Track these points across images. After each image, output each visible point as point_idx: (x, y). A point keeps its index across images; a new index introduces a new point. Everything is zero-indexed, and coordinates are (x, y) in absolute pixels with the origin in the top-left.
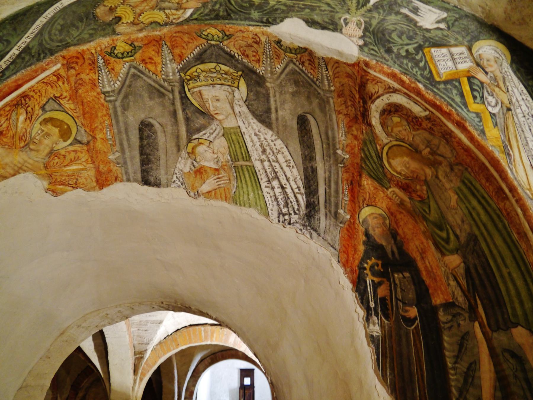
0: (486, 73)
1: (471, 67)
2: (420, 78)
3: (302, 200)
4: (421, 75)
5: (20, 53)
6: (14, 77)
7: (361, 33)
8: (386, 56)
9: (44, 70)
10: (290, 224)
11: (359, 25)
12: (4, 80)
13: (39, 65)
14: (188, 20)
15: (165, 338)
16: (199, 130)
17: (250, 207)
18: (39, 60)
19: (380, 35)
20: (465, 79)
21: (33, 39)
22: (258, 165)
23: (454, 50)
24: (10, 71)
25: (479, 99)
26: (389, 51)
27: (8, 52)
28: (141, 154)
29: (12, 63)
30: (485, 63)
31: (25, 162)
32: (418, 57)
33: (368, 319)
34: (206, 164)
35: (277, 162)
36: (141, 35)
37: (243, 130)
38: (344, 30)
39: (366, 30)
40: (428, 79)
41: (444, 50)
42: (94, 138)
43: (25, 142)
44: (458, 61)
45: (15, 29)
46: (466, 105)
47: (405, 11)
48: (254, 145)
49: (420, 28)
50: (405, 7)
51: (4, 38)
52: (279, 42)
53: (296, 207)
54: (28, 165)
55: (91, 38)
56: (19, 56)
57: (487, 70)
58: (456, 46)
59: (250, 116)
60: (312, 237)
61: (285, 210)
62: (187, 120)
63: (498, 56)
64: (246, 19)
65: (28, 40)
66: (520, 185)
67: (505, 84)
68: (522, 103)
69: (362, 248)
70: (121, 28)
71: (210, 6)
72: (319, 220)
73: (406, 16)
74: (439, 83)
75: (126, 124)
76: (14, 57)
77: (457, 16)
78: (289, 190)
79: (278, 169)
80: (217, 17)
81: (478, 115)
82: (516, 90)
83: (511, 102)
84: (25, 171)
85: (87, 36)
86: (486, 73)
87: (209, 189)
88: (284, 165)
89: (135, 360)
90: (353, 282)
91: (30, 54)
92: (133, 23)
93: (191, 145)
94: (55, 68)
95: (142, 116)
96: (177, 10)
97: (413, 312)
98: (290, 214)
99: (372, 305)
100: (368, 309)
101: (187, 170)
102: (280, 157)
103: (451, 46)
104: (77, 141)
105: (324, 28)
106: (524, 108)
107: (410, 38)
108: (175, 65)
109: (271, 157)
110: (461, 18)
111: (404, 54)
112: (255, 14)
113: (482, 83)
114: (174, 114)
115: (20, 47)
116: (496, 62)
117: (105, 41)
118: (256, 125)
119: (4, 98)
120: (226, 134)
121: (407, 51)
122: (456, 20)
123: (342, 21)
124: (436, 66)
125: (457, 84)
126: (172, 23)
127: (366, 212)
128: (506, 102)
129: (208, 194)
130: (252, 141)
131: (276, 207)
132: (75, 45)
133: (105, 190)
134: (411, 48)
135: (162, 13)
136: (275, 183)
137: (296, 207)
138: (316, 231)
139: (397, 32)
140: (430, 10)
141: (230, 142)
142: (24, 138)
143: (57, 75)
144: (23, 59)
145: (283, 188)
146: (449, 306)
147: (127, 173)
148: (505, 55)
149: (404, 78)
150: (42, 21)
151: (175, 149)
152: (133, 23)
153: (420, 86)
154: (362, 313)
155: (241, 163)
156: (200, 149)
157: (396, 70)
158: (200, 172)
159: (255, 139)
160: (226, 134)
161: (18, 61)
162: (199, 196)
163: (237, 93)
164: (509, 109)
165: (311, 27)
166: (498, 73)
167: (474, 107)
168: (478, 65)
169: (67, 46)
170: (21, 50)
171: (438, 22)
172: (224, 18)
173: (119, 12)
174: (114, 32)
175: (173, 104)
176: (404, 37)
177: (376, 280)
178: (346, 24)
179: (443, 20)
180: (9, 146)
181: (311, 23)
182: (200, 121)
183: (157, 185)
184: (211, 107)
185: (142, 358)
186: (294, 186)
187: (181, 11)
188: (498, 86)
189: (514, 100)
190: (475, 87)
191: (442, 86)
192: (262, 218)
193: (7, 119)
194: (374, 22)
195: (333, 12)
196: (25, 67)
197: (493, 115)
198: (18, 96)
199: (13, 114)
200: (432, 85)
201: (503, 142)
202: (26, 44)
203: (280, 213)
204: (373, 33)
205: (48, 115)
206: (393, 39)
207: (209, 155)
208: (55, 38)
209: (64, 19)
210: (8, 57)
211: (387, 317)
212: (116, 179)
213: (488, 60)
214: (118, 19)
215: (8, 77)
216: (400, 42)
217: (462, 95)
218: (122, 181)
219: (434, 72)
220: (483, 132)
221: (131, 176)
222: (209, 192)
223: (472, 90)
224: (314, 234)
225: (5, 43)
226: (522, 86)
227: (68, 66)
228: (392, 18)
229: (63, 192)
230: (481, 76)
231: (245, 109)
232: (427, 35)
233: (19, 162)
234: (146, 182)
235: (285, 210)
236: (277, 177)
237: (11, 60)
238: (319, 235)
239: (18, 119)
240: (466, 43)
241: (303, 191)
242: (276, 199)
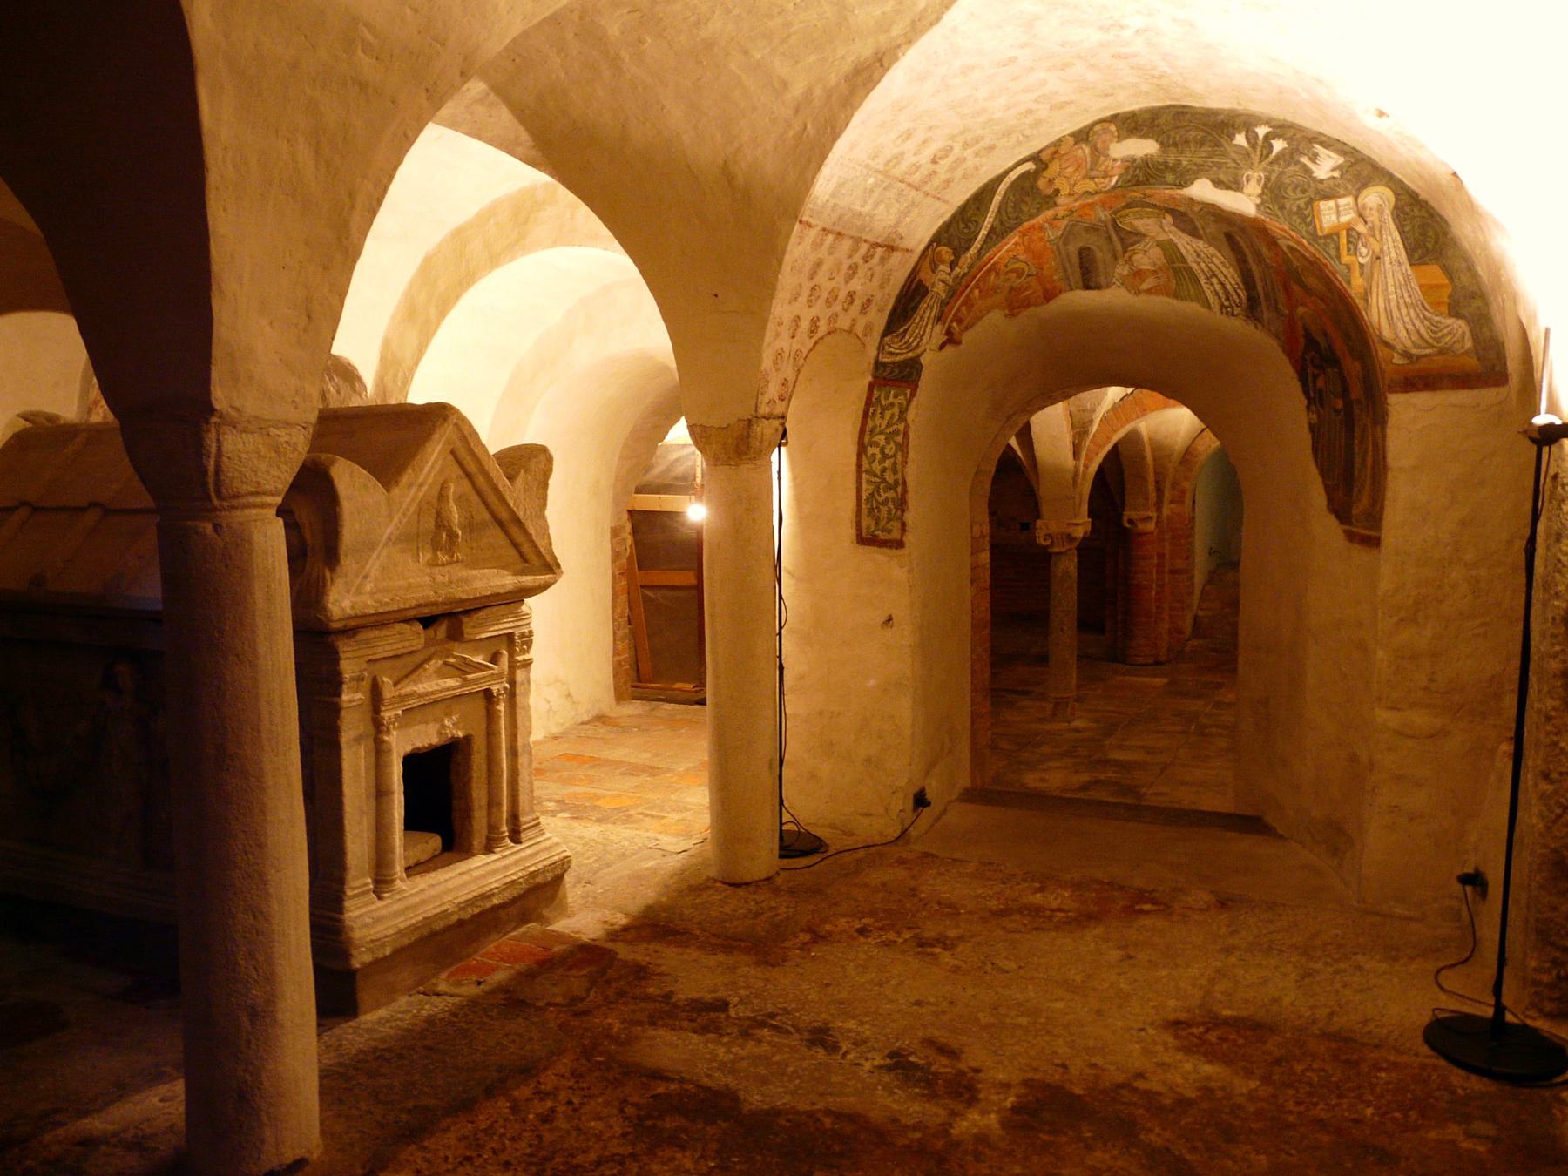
0: (1366, 222)
1: (1352, 219)
2: (1304, 234)
3: (1243, 294)
4: (1307, 232)
5: (989, 233)
6: (988, 255)
7: (1259, 190)
8: (1279, 213)
9: (1006, 244)
10: (1233, 315)
11: (1259, 181)
13: (1005, 240)
14: (1114, 188)
15: (1122, 399)
16: (1133, 245)
17: (1192, 301)
18: (1003, 238)
19: (1276, 191)
20: (1344, 232)
21: (994, 220)
22: (1194, 266)
23: (1342, 201)
25: (1352, 252)
26: (1282, 208)
27: (978, 233)
28: (1081, 268)
29: (985, 242)
30: (1367, 212)
32: (1306, 212)
33: (1308, 408)
34: (1143, 267)
35: (1213, 262)
36: (1077, 204)
37: (1176, 241)
38: (1245, 190)
39: (1265, 187)
40: (1311, 235)
41: (1331, 203)
42: (1042, 269)
44: (1342, 213)
45: (978, 209)
46: (1339, 257)
47: (1304, 160)
48: (1188, 251)
49: (1314, 179)
50: (1305, 154)
52: (1191, 199)
53: (1238, 301)
55: (1039, 211)
56: (988, 236)
57: (1368, 220)
58: (1344, 196)
59: (1181, 233)
60: (1256, 328)
61: (1226, 303)
62: (1121, 240)
63: (1381, 202)
64: (1161, 184)
65: (991, 220)
66: (1372, 325)
67: (1381, 231)
68: (1392, 250)
69: (1302, 340)
70: (1061, 200)
71: (1131, 173)
72: (1262, 311)
73: (1305, 165)
74: (1321, 237)
75: (1068, 255)
77: (1353, 160)
78: (1228, 287)
79: (1214, 268)
80: (1138, 183)
81: (1348, 267)
82: (1390, 238)
83: (1382, 250)
85: (1035, 211)
86: (1366, 222)
87: (1149, 286)
88: (1220, 266)
89: (1074, 436)
90: (1297, 371)
91: (995, 233)
92: (1070, 195)
93: (1127, 255)
94: (1014, 241)
95: (1081, 244)
96: (1104, 178)
97: (1340, 405)
98: (1232, 308)
99: (1312, 395)
100: (1308, 397)
101: (1125, 273)
102: (1214, 259)
103: (1339, 197)
104: (1029, 275)
105: (1228, 188)
106: (1393, 255)
107: (1304, 191)
108: (1106, 212)
109: (1207, 260)
110: (1355, 163)
111: (1295, 209)
112: (1170, 177)
113: (1359, 234)
114: (1109, 239)
116: (1378, 210)
117: (1050, 213)
118: (1187, 238)
120: (1159, 244)
121: (1298, 207)
122: (1351, 166)
123: (1244, 179)
124: (1321, 221)
125: (1335, 237)
126: (1101, 192)
127: (1301, 310)
128: (1377, 250)
129: (1149, 291)
130: (1185, 248)
131: (1217, 301)
132: (1028, 220)
133: (1052, 302)
134: (1302, 203)
135: (1092, 182)
136: (1214, 280)
137: (1238, 301)
138: (1260, 322)
139: (1292, 186)
140: (1328, 156)
141: (1164, 250)
143: (1016, 244)
144: (992, 239)
145: (1223, 284)
146: (1359, 402)
147: (1070, 286)
148: (1389, 201)
149: (1293, 234)
150: (998, 198)
151: (1112, 260)
152: (1070, 195)
153: (1304, 241)
154: (1306, 402)
155: (1177, 265)
156: (1136, 257)
157: (1286, 228)
158: (1139, 274)
159: (1188, 247)
160: (1159, 244)
162: (1139, 292)
163: (1164, 221)
164: (1378, 258)
165: (1216, 187)
166: (1377, 223)
167: (1346, 258)
168: (1360, 215)
169: (1020, 224)
171: (1333, 170)
172: (1144, 184)
173: (1057, 184)
174: (1055, 205)
175: (1107, 232)
176: (1298, 191)
177: (1316, 372)
178: (1248, 181)
179: (1339, 167)
181: (1218, 183)
182: (1134, 239)
183: (1098, 287)
184: (1142, 230)
185: (1086, 433)
186: (1233, 283)
187: (1107, 180)
188: (1374, 236)
189: (1385, 248)
190: (1352, 240)
191: (1323, 241)
192: (1204, 310)
194: (1273, 177)
195: (1236, 168)
196: (994, 245)
197: (1361, 266)
200: (1314, 240)
201: (1365, 289)
203: (1222, 305)
204: (1272, 192)
205: (1010, 268)
206: (1287, 194)
207: (1145, 260)
208: (1011, 216)
209: (1014, 196)
210: (980, 237)
211: (1322, 405)
212: (1060, 292)
213: (1371, 209)
214: (1057, 191)
216: (1295, 196)
217: (1338, 249)
218: (1066, 291)
219: (1318, 227)
220: (1349, 282)
221: (1073, 284)
222: (1151, 289)
223: (1349, 242)
224: (1260, 326)
226: (1397, 233)
227: (1023, 235)
228: (1292, 168)
229: (1018, 314)
230: (1361, 228)
231: (1174, 228)
232: (1321, 186)
234: (1087, 287)
235: (1226, 303)
236: (1214, 275)
238: (1263, 326)
240: (1354, 192)
241: (1241, 285)
242: (1217, 294)
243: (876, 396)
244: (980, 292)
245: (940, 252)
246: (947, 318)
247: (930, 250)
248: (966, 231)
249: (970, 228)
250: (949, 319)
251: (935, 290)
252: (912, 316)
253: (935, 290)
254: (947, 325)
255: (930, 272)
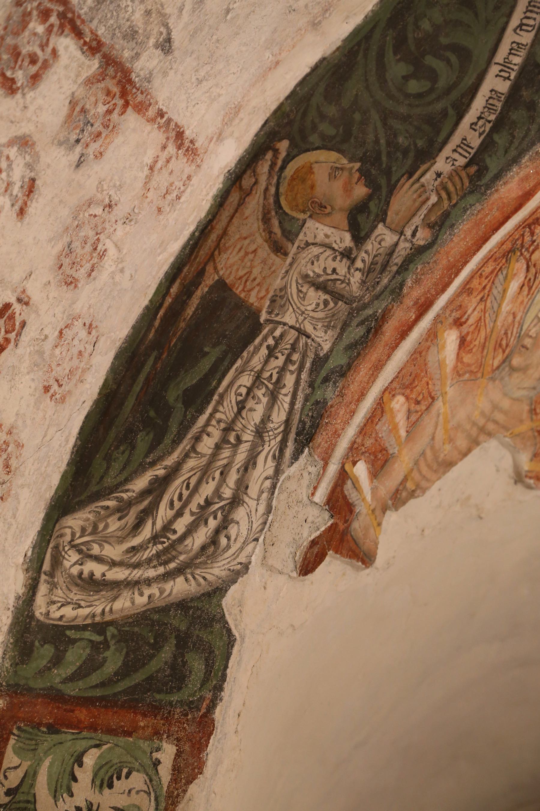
5: (515, 89)
12: (488, 186)
24: (501, 152)
29: (497, 126)
31: (495, 407)
43: (504, 352)
51: (444, 41)
54: (499, 417)
65: (527, 38)
76: (499, 105)
84: (490, 435)
115: (506, 65)
119: (485, 239)
142: (504, 343)
161: (514, 116)
170: (513, 75)
180: (471, 372)
193: (481, 299)
198: (517, 228)
199: (497, 281)
202: (523, 53)
215: (498, 177)
225: (454, 59)
233: (483, 414)
237: (493, 117)
239: (505, 291)
243: (14, 779)
244: (463, 342)
245: (309, 169)
246: (337, 435)
247: (264, 168)
248: (414, 86)
249: (433, 76)
250: (343, 445)
251: (289, 318)
252: (184, 428)
253: (289, 318)
254: (333, 468)
255: (265, 251)
